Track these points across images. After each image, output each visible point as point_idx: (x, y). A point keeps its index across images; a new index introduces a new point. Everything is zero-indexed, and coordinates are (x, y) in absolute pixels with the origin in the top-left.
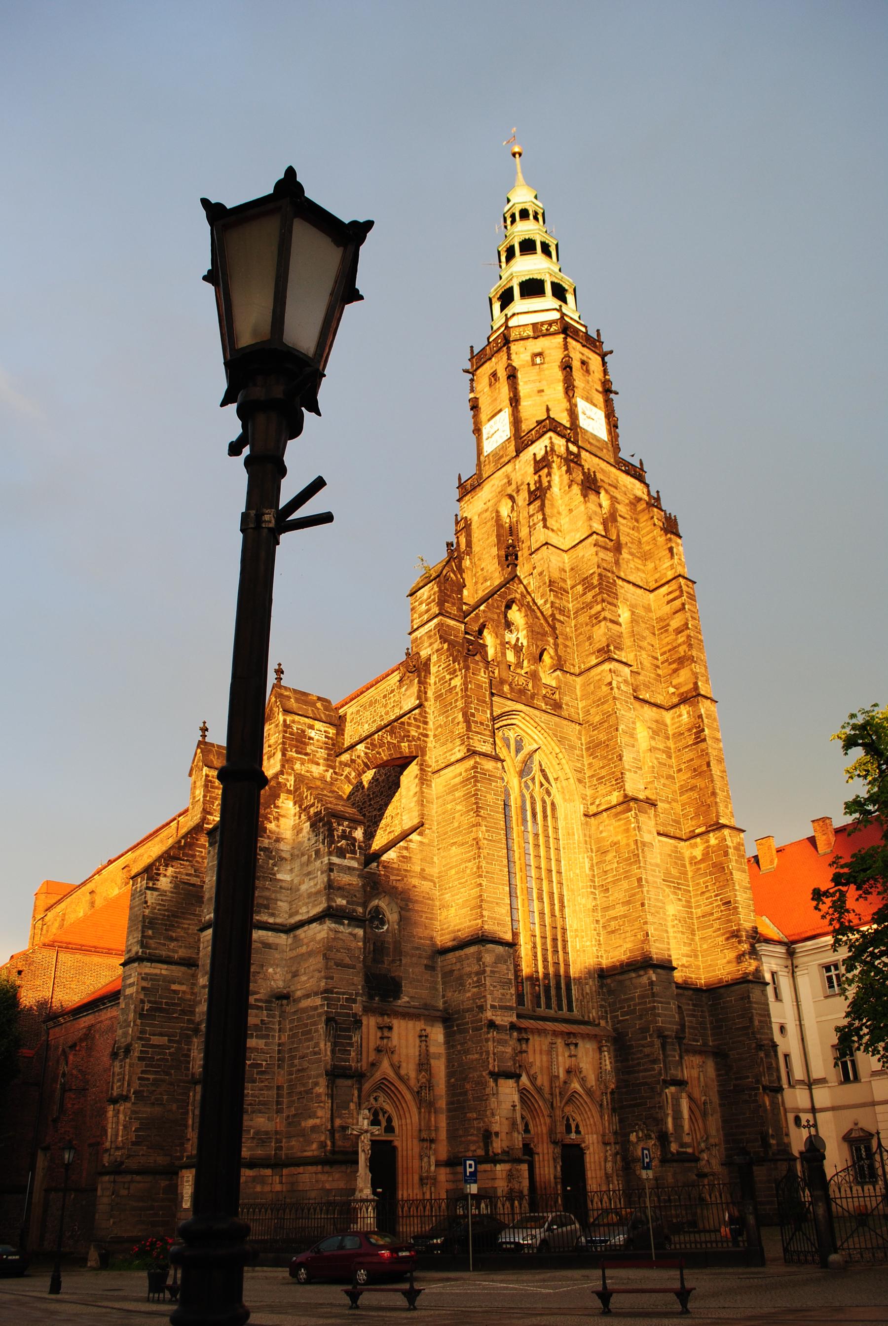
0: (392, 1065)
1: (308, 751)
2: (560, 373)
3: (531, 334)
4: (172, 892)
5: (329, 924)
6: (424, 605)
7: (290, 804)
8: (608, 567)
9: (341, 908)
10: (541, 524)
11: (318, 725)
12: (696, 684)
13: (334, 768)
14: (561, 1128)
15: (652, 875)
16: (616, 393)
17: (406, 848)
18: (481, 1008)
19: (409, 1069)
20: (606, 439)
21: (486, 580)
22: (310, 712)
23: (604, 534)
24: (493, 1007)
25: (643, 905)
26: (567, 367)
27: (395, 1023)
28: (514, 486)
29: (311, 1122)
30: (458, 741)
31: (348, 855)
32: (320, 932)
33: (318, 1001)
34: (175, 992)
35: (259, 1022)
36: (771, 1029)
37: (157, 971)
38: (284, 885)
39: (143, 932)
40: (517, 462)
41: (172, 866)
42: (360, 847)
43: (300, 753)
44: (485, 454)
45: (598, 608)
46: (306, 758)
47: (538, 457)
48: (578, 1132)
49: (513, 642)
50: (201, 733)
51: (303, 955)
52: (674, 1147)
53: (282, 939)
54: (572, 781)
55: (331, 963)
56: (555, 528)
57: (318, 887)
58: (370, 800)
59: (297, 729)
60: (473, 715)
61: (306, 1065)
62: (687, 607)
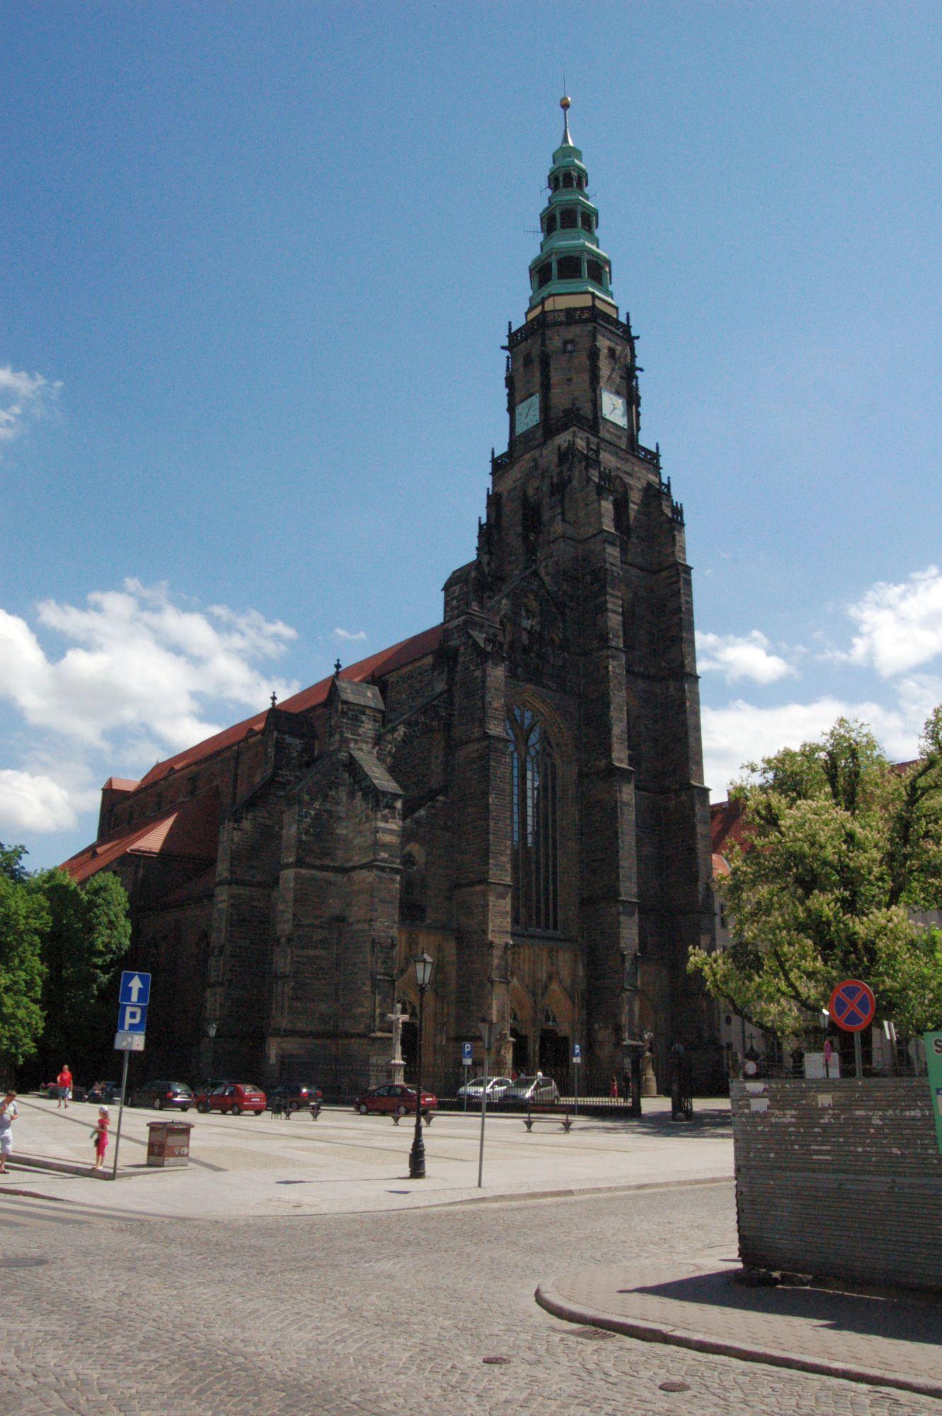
3: (564, 319)
7: (346, 775)
8: (614, 562)
10: (559, 517)
12: (682, 662)
14: (541, 1017)
16: (641, 370)
17: (433, 807)
18: (485, 932)
20: (626, 427)
21: (511, 555)
25: (618, 852)
28: (540, 471)
29: (360, 1010)
30: (477, 724)
31: (390, 820)
43: (354, 735)
44: (517, 434)
46: (358, 738)
47: (563, 448)
48: (554, 1021)
50: (271, 701)
53: (339, 878)
54: (570, 746)
55: (377, 900)
58: (405, 759)
61: (356, 970)
62: (682, 591)
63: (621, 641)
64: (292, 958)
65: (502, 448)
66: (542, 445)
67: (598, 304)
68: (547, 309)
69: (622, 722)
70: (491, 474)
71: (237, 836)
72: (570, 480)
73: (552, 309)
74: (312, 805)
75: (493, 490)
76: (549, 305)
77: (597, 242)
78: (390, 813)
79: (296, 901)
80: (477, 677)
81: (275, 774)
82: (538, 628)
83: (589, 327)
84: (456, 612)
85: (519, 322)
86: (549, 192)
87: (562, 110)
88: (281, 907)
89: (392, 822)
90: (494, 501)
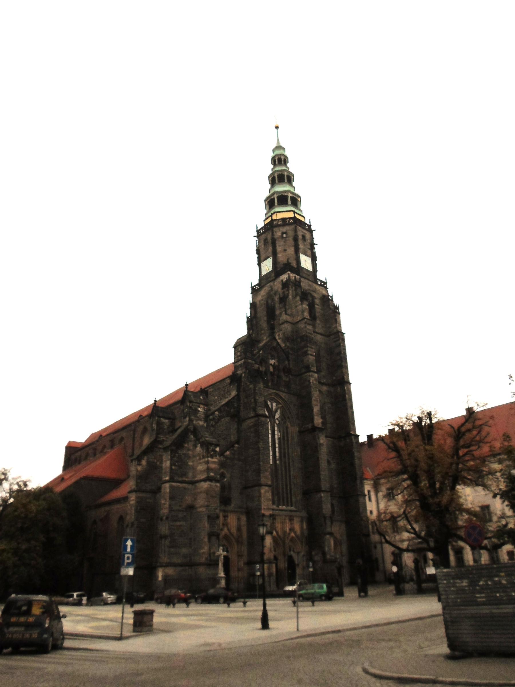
0: (228, 530)
1: (198, 416)
2: (293, 243)
6: (239, 353)
7: (192, 436)
9: (212, 477)
10: (284, 312)
11: (201, 406)
15: (323, 456)
16: (317, 244)
18: (260, 509)
19: (234, 530)
20: (312, 271)
22: (199, 401)
23: (309, 317)
24: (264, 509)
26: (296, 239)
27: (229, 514)
28: (274, 292)
29: (202, 551)
32: (205, 485)
36: (366, 512)
40: (275, 281)
44: (262, 275)
45: (306, 349)
49: (273, 364)
52: (328, 557)
53: (190, 486)
56: (290, 314)
59: (194, 408)
60: (257, 399)
62: (341, 344)
63: (315, 368)
64: (169, 526)
65: (256, 281)
66: (274, 280)
67: (297, 216)
68: (273, 219)
69: (317, 405)
70: (251, 293)
71: (139, 468)
72: (288, 296)
73: (276, 219)
75: (252, 301)
76: (274, 217)
77: (294, 187)
80: (251, 388)
81: (157, 437)
82: (277, 364)
83: (293, 227)
84: (240, 358)
85: (261, 225)
86: (272, 166)
87: (276, 129)
88: (163, 502)
90: (253, 306)
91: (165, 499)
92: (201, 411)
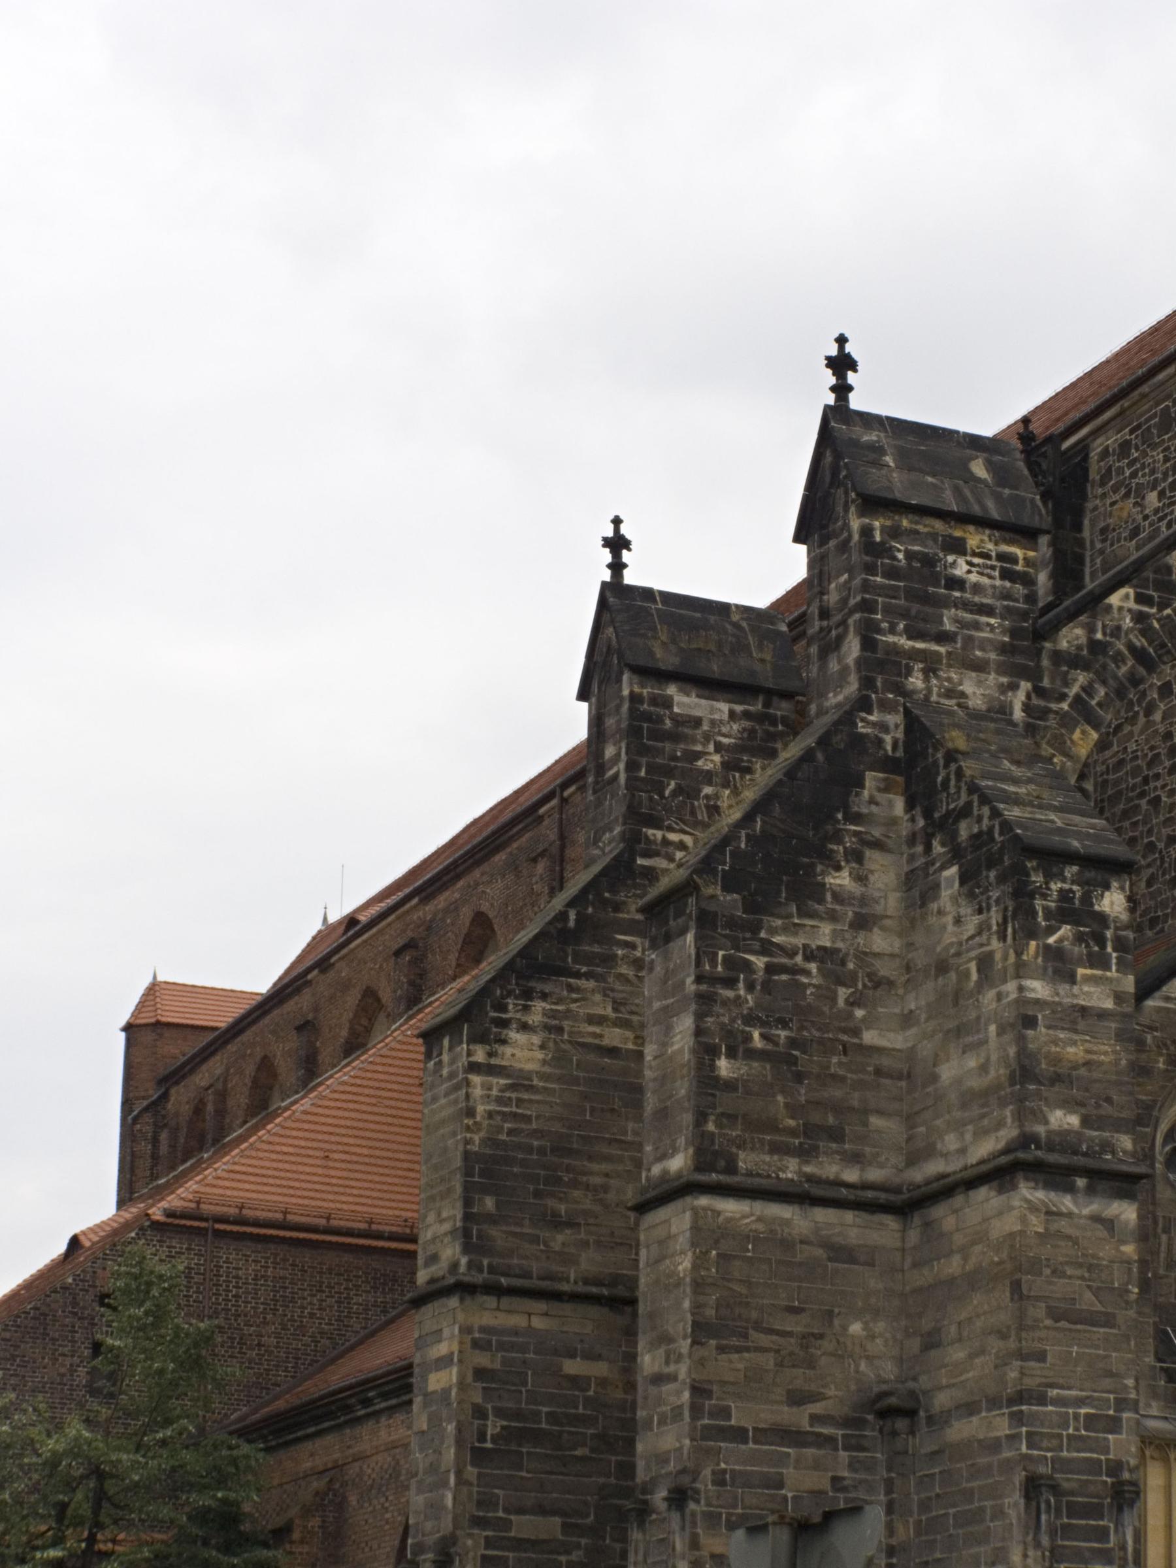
1: (948, 626)
4: (543, 1077)
5: (1028, 1192)
9: (1062, 1142)
11: (974, 539)
13: (1034, 675)
22: (948, 494)
31: (1081, 971)
33: (1002, 1426)
34: (575, 1381)
35: (826, 1485)
37: (517, 1321)
38: (886, 1062)
39: (467, 1202)
41: (544, 996)
42: (1120, 945)
46: (942, 650)
50: (606, 556)
51: (951, 1281)
55: (1038, 1311)
57: (992, 1073)
59: (909, 555)
74: (755, 928)
78: (1079, 938)
79: (701, 1330)
81: (634, 843)
89: (1088, 979)
91: (665, 1339)
92: (977, 588)
